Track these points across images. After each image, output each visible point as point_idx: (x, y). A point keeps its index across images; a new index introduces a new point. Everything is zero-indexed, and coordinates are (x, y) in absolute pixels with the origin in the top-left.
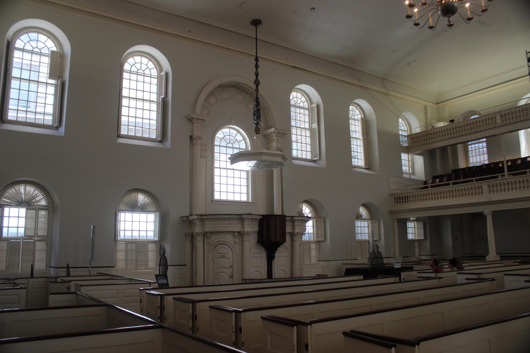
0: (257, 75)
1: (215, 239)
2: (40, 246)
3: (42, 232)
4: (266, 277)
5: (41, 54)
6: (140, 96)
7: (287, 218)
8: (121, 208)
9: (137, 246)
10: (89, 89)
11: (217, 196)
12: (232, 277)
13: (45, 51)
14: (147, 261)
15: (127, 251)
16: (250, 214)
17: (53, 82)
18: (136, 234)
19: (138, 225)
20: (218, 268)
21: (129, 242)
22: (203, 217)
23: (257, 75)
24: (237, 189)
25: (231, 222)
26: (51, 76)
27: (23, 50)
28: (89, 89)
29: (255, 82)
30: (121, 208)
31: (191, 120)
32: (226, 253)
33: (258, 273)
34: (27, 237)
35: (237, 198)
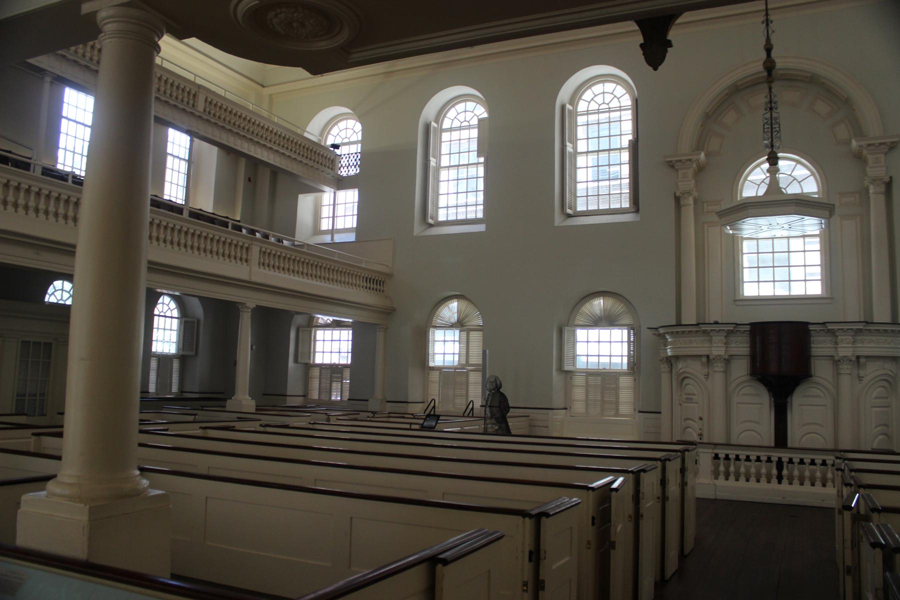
0: (769, 49)
1: (680, 366)
2: (475, 378)
3: (476, 358)
4: (773, 444)
5: (469, 127)
6: (604, 145)
7: (811, 328)
8: (577, 322)
9: (604, 378)
10: (525, 157)
11: (750, 290)
12: (701, 435)
13: (475, 122)
14: (617, 403)
15: (587, 386)
16: (716, 323)
17: (482, 160)
18: (605, 360)
19: (602, 347)
20: (686, 419)
21: (590, 374)
22: (662, 331)
23: (769, 49)
24: (797, 273)
25: (693, 339)
26: (478, 156)
27: (451, 130)
28: (525, 157)
29: (764, 63)
30: (577, 322)
31: (671, 165)
32: (694, 394)
33: (752, 433)
34: (462, 366)
35: (798, 290)
